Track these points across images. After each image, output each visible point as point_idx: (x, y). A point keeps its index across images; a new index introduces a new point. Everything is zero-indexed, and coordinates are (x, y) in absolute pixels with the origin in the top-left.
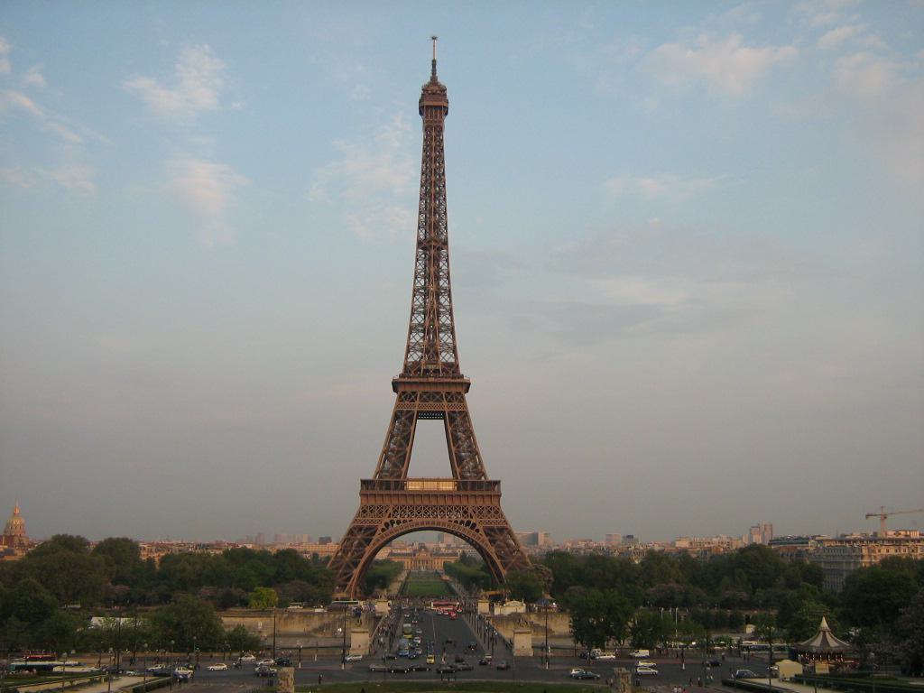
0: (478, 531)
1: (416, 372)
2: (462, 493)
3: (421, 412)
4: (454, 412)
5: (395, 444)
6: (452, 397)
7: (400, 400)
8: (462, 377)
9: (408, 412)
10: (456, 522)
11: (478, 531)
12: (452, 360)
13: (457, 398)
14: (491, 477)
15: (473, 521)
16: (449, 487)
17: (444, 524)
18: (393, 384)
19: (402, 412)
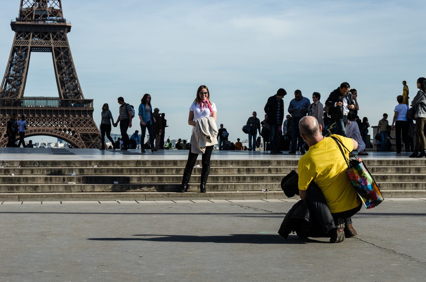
0: (76, 136)
1: (29, 17)
2: (64, 109)
3: (34, 47)
4: (59, 48)
5: (14, 70)
6: (57, 36)
7: (17, 37)
8: (63, 21)
9: (23, 47)
10: (60, 130)
11: (76, 136)
12: (57, 8)
13: (61, 37)
14: (86, 96)
15: (73, 129)
16: (55, 104)
17: (52, 131)
18: (11, 24)
19: (19, 47)
